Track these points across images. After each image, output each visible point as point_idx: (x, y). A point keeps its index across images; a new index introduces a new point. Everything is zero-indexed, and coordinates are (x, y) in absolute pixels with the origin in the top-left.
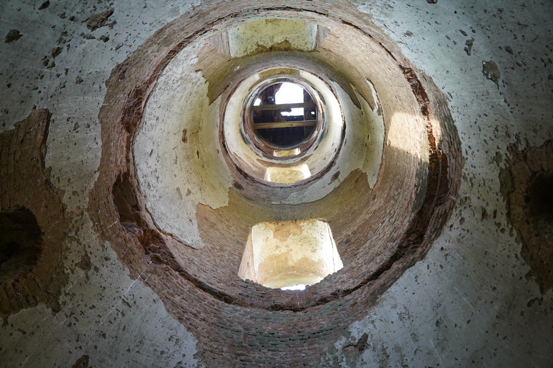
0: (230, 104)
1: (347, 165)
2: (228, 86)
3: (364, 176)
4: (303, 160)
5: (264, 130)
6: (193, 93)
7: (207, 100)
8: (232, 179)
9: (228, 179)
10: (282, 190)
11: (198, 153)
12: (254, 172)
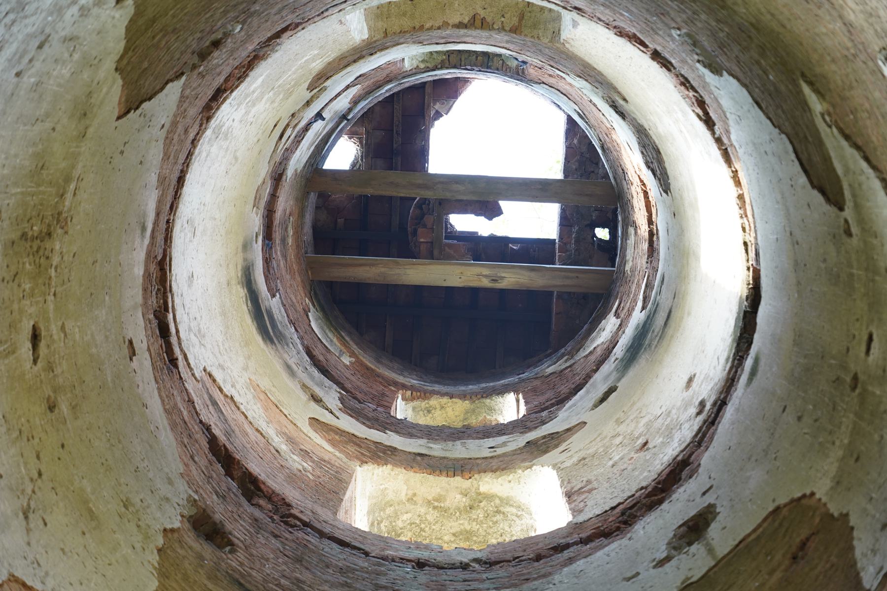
0: (217, 134)
1: (756, 476)
2: (216, 44)
3: (837, 530)
4: (537, 449)
5: (359, 288)
6: (55, 38)
7: (113, 91)
8: (182, 486)
9: (164, 490)
10: (423, 576)
11: (35, 338)
12: (294, 478)
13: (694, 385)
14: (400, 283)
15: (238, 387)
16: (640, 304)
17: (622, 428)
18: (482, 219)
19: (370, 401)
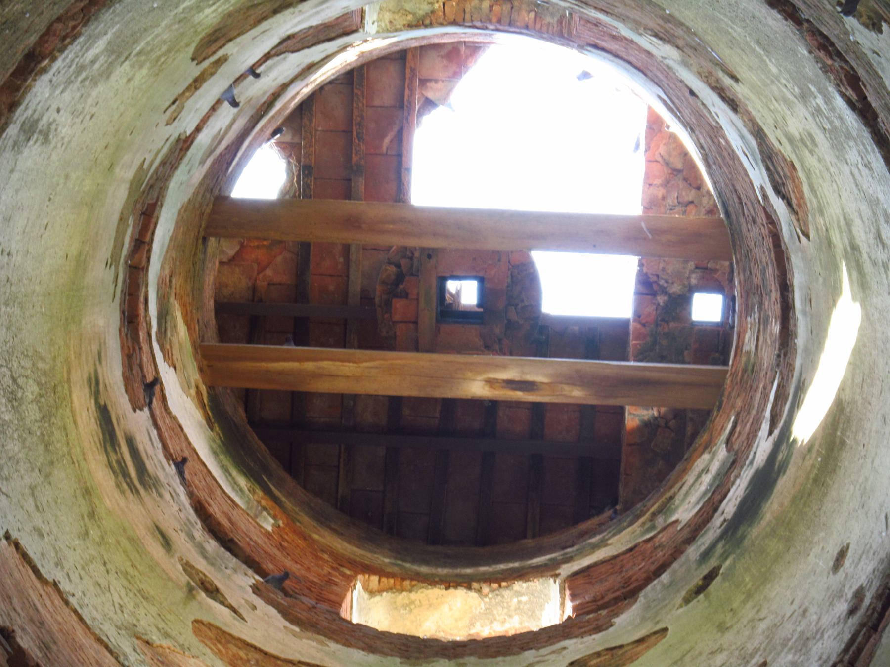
13: (847, 562)
15: (67, 566)
16: (765, 427)
17: (729, 637)
19: (306, 592)
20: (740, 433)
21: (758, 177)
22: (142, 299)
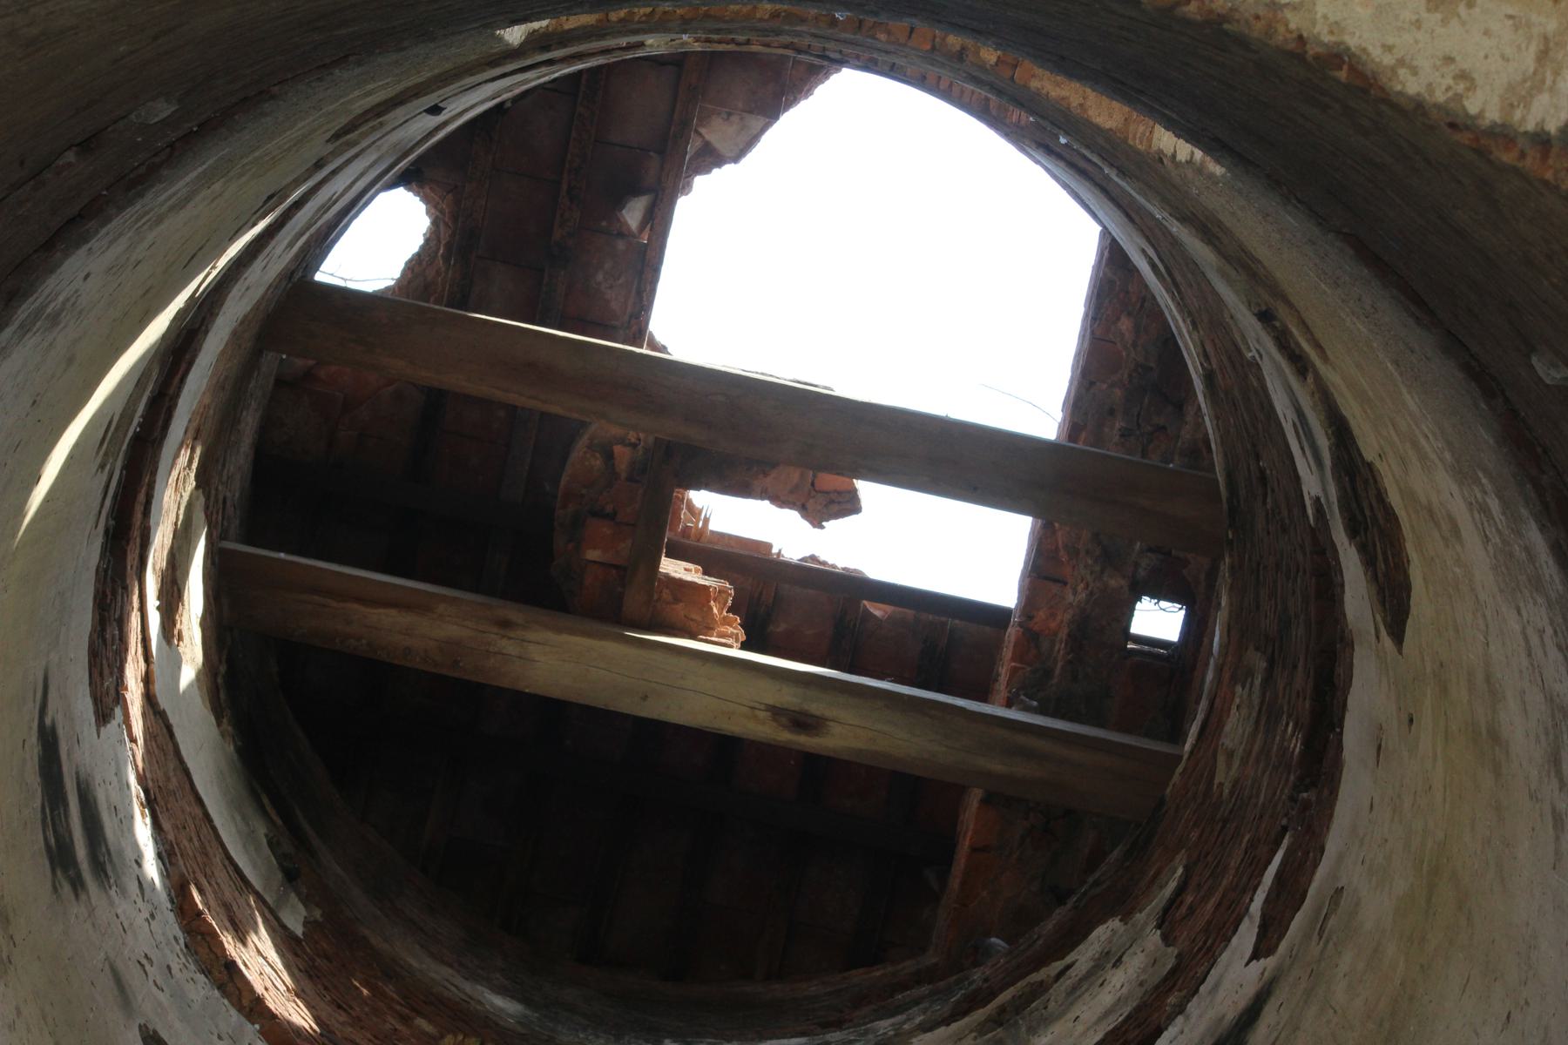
14: (505, 683)
16: (1246, 936)
18: (792, 517)
20: (1192, 910)
21: (1315, 483)
22: (142, 497)
